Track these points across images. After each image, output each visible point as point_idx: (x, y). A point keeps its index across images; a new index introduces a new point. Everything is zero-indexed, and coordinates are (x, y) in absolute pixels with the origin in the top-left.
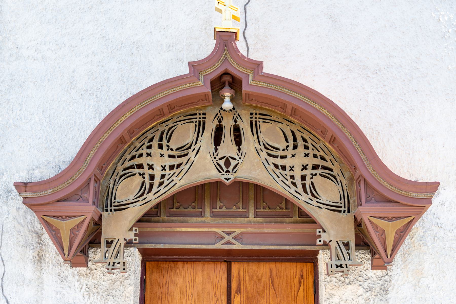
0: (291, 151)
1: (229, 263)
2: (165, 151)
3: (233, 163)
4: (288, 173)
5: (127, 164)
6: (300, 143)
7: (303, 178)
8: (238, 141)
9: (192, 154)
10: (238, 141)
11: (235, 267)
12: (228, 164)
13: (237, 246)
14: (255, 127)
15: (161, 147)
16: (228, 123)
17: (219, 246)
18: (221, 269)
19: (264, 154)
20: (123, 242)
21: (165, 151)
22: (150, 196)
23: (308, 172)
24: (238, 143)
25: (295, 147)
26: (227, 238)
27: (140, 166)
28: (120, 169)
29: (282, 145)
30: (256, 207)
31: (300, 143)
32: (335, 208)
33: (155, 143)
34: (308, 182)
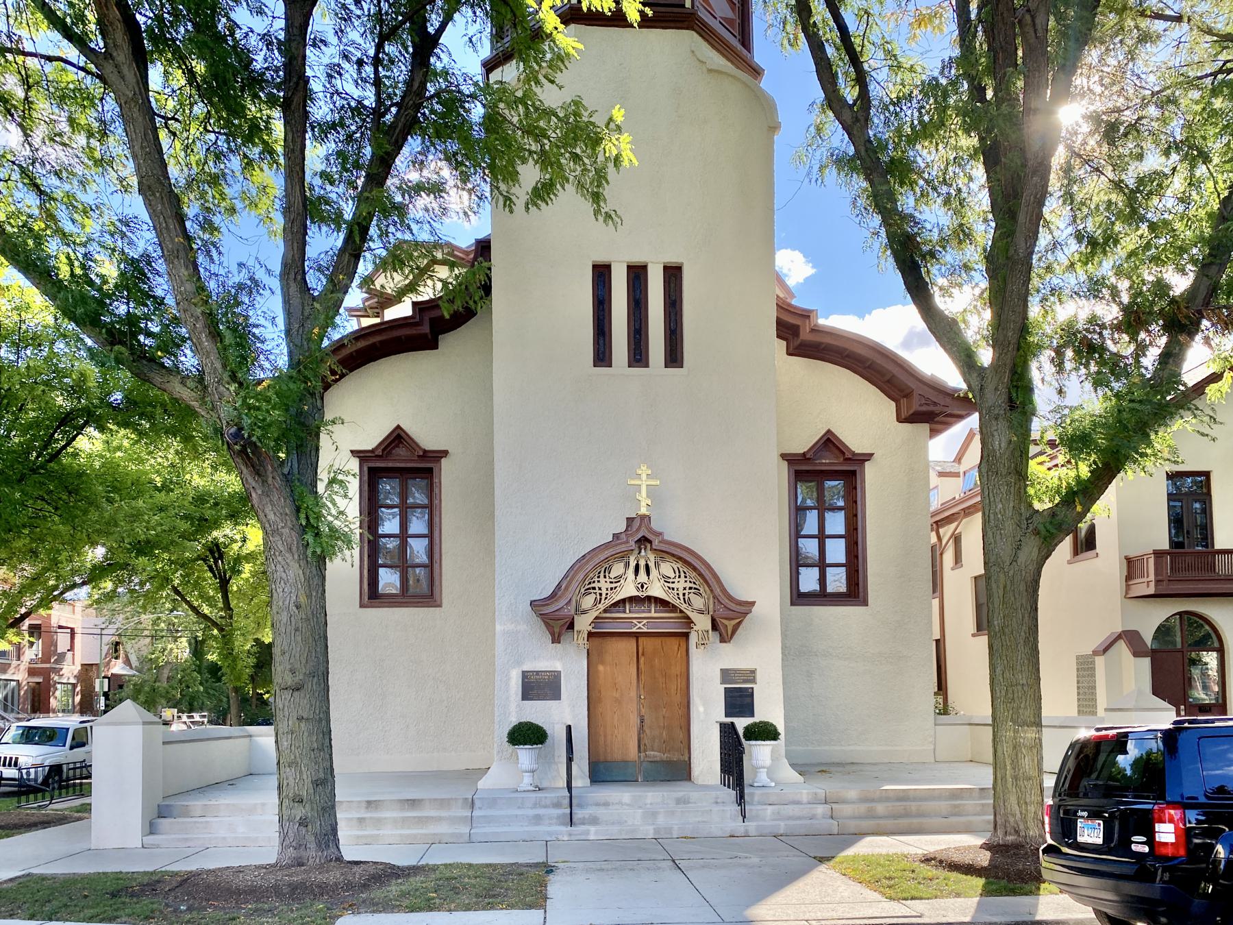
0: (677, 579)
1: (637, 638)
2: (607, 579)
3: (645, 586)
4: (675, 591)
5: (587, 587)
6: (682, 575)
7: (684, 594)
8: (648, 573)
9: (622, 581)
10: (648, 574)
11: (641, 640)
12: (642, 587)
13: (646, 630)
14: (657, 565)
15: (605, 577)
16: (642, 563)
17: (634, 630)
18: (633, 641)
19: (662, 581)
20: (586, 633)
21: (607, 579)
22: (600, 606)
23: (687, 592)
24: (648, 574)
25: (679, 577)
26: (639, 625)
27: (594, 588)
28: (583, 590)
29: (672, 575)
30: (656, 607)
31: (682, 575)
32: (701, 612)
33: (602, 574)
34: (686, 597)
